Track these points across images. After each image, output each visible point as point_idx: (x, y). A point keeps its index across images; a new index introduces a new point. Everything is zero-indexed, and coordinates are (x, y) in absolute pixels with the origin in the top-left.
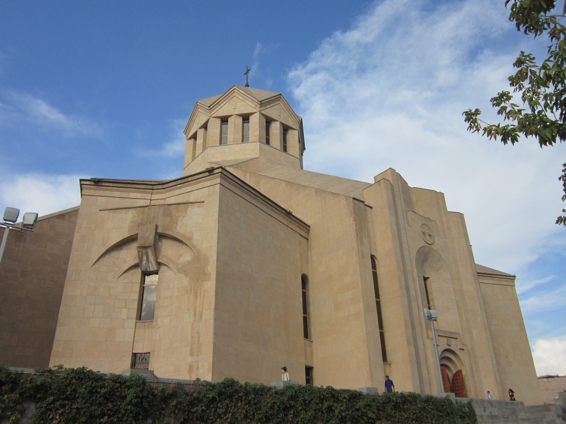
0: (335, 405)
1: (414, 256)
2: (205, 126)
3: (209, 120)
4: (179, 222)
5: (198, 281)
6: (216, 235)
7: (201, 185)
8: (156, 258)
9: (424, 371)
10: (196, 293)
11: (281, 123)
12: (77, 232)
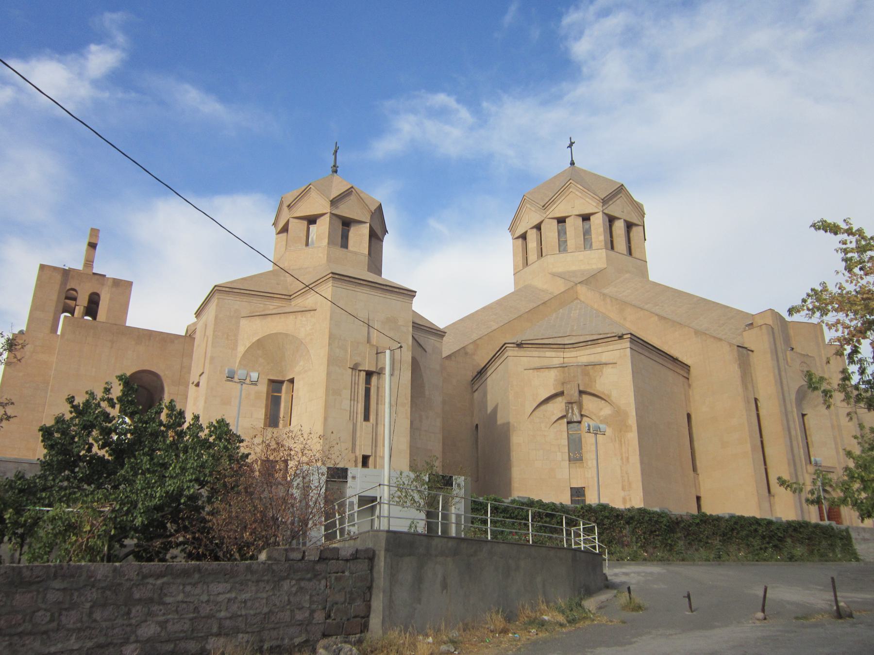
0: (759, 528)
1: (793, 396)
2: (538, 227)
4: (597, 381)
5: (621, 432)
7: (611, 347)
8: (580, 411)
10: (621, 441)
11: (625, 221)
12: (511, 390)
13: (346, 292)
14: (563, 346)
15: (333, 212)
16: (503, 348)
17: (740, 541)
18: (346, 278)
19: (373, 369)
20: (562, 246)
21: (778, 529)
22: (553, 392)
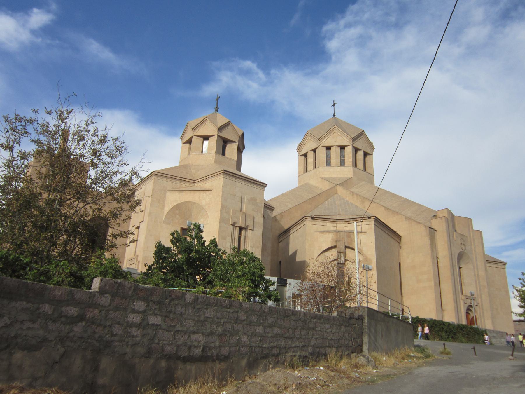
1: (456, 257)
2: (315, 151)
3: (318, 147)
6: (374, 250)
9: (460, 315)
13: (230, 181)
14: (336, 221)
15: (219, 135)
16: (303, 219)
17: (435, 333)
18: (231, 174)
19: (243, 226)
20: (328, 163)
21: (453, 328)
22: (330, 246)
